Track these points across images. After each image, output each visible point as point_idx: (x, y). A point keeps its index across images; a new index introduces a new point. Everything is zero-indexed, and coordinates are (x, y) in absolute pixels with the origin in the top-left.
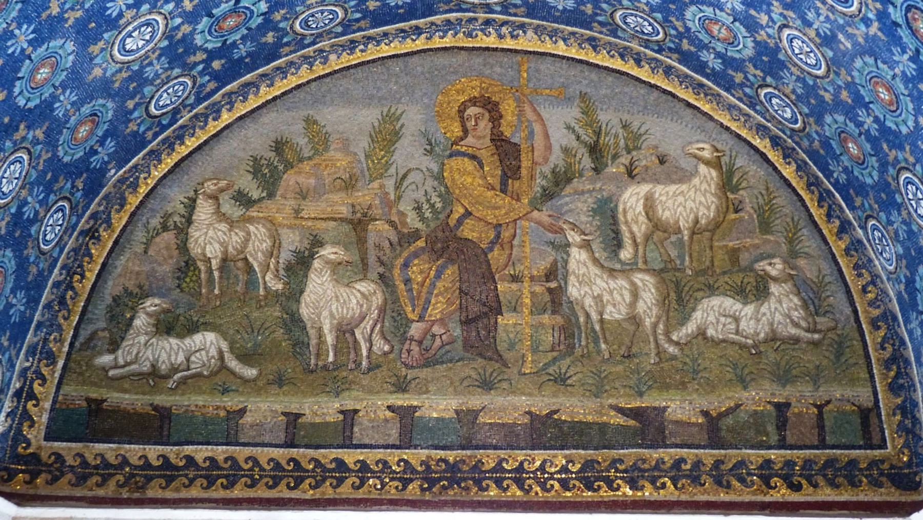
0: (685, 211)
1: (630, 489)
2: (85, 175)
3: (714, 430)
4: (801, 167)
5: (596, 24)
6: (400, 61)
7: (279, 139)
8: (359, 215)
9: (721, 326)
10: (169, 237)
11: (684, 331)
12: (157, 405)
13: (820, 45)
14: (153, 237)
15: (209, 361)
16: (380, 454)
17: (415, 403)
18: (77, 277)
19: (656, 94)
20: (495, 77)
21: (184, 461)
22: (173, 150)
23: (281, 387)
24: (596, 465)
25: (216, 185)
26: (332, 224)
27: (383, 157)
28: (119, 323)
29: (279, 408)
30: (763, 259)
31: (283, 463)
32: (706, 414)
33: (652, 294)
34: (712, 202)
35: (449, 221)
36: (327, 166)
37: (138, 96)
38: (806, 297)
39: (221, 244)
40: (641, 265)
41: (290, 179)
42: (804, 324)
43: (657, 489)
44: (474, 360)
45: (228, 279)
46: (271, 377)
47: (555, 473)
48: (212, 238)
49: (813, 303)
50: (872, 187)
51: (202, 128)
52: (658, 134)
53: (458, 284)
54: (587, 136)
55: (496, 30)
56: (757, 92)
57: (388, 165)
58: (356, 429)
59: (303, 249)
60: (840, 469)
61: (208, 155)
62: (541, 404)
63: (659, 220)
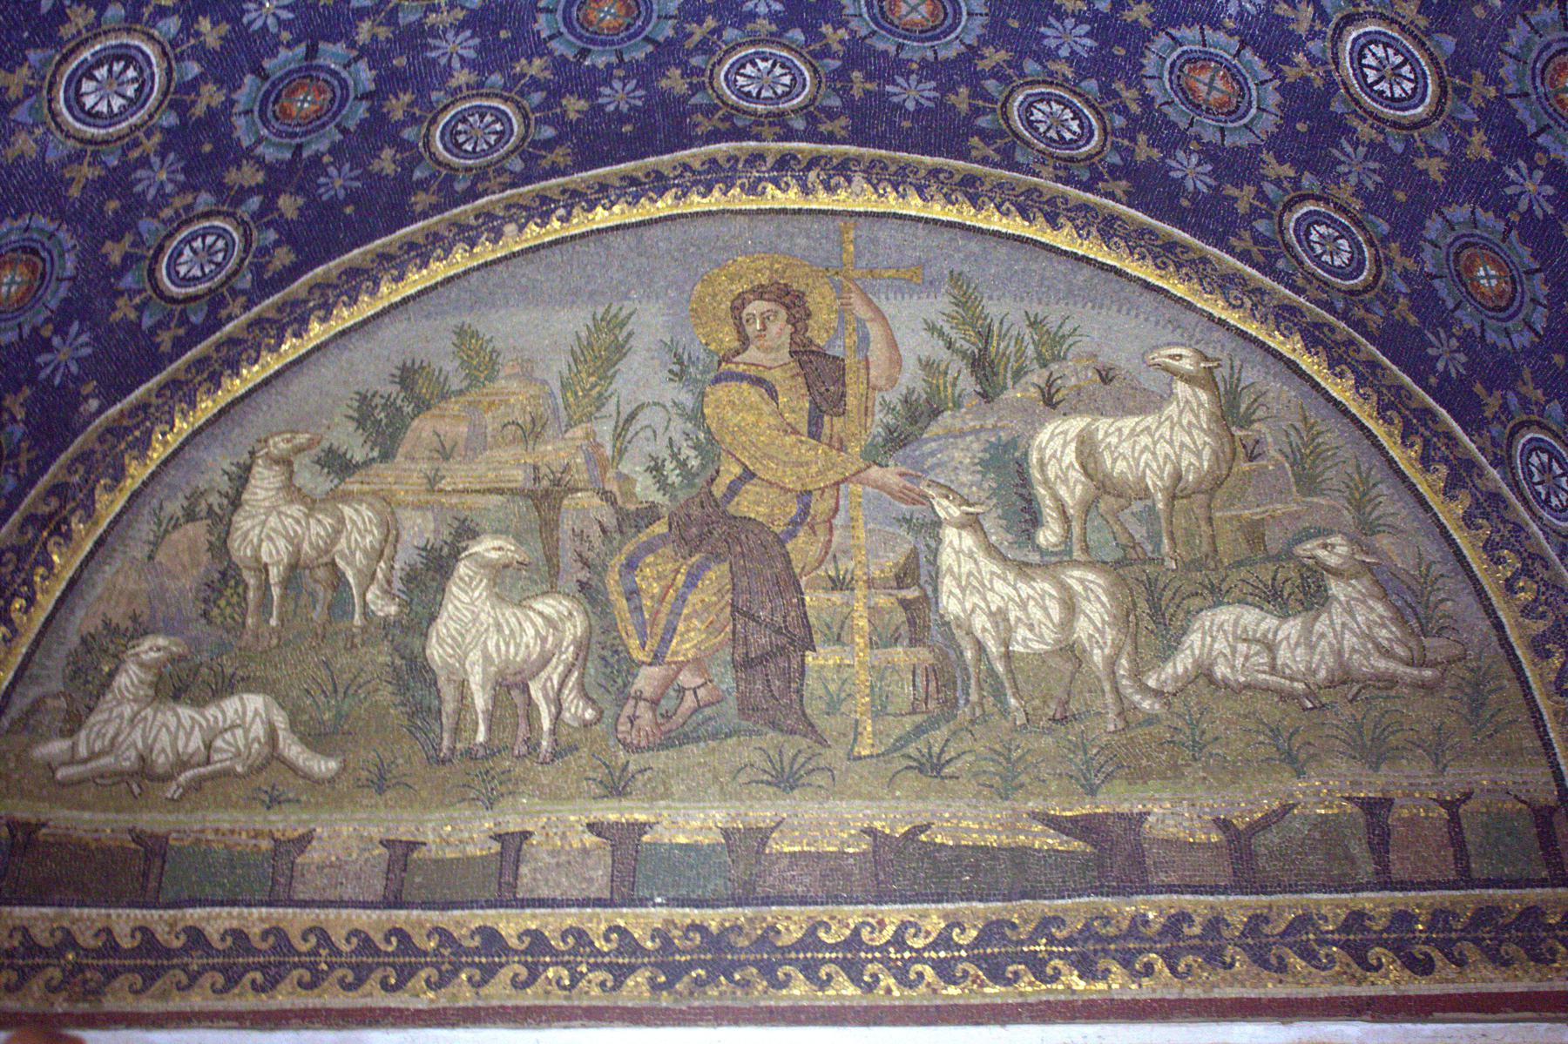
0: (1156, 459)
1: (1081, 977)
2: (27, 391)
3: (1242, 857)
4: (1367, 375)
5: (975, 140)
6: (630, 236)
7: (409, 363)
8: (545, 483)
9: (1239, 661)
11: (1170, 670)
12: (142, 831)
13: (1427, 33)
14: (166, 531)
15: (248, 746)
16: (570, 917)
17: (641, 817)
18: (18, 603)
19: (1087, 271)
20: (798, 252)
21: (183, 937)
22: (219, 386)
23: (381, 791)
24: (1008, 932)
26: (496, 499)
27: (594, 386)
28: (87, 682)
29: (376, 832)
30: (1309, 537)
31: (378, 938)
32: (1224, 825)
33: (1103, 605)
34: (1205, 443)
35: (714, 489)
36: (491, 404)
37: (128, 238)
38: (1399, 603)
39: (289, 540)
40: (1077, 554)
41: (423, 428)
42: (1400, 651)
43: (1136, 975)
44: (759, 733)
45: (297, 597)
46: (365, 774)
47: (924, 949)
48: (274, 530)
49: (1416, 613)
50: (1528, 352)
51: (274, 349)
52: (1095, 334)
53: (728, 597)
54: (966, 341)
55: (798, 179)
56: (1280, 223)
57: (601, 401)
58: (524, 870)
59: (437, 546)
60: (1507, 928)
62: (892, 817)
63: (1108, 476)
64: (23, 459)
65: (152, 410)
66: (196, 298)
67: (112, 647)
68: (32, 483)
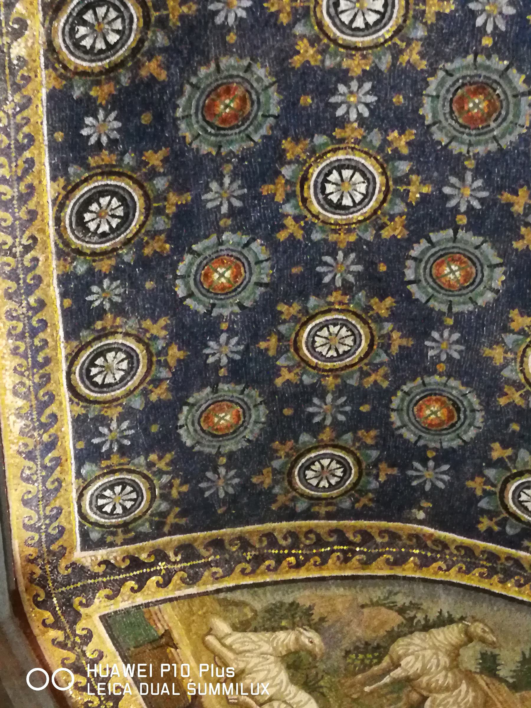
10: (395, 619)
18: (292, 559)
22: (489, 577)
25: (484, 632)
28: (269, 619)
37: (509, 452)
45: (392, 692)
61: (510, 611)
64: (364, 501)
65: (447, 552)
66: (518, 519)
67: (298, 619)
68: (358, 516)
